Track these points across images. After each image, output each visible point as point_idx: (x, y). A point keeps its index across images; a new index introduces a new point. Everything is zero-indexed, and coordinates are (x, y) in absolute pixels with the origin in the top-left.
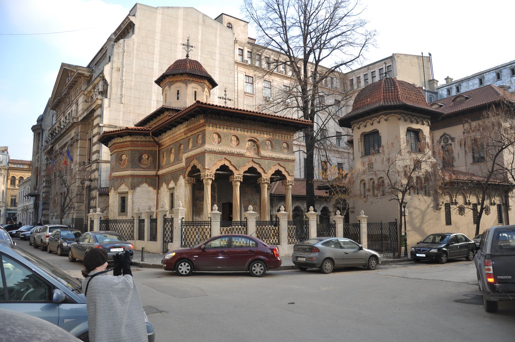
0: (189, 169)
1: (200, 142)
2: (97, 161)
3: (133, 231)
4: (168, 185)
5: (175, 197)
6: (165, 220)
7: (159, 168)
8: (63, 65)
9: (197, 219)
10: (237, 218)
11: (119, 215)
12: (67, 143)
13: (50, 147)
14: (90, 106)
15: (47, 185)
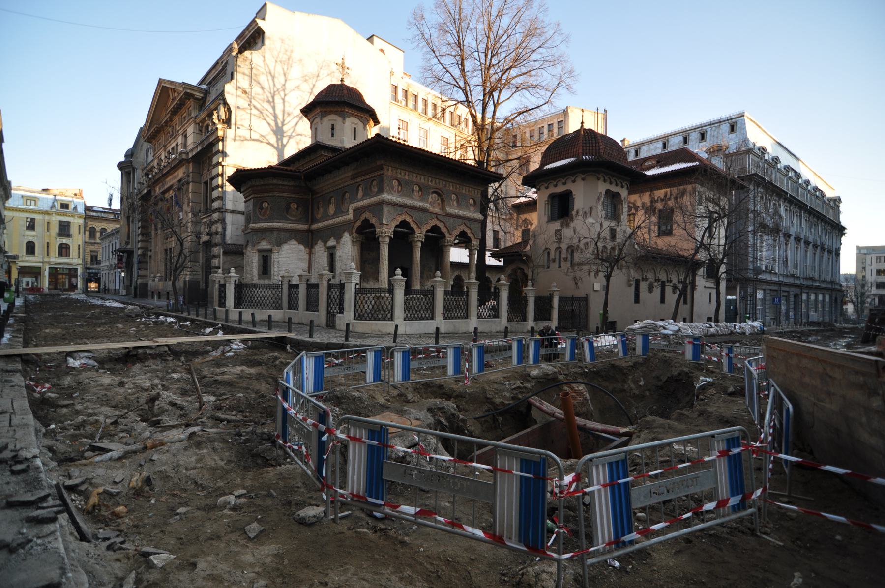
0: (359, 223)
1: (375, 190)
2: (220, 210)
3: (281, 299)
4: (325, 243)
5: (337, 258)
6: (330, 286)
7: (314, 221)
8: (161, 81)
9: (371, 285)
10: (417, 286)
11: (259, 279)
12: (172, 186)
13: (145, 191)
14: (207, 138)
15: (144, 239)
